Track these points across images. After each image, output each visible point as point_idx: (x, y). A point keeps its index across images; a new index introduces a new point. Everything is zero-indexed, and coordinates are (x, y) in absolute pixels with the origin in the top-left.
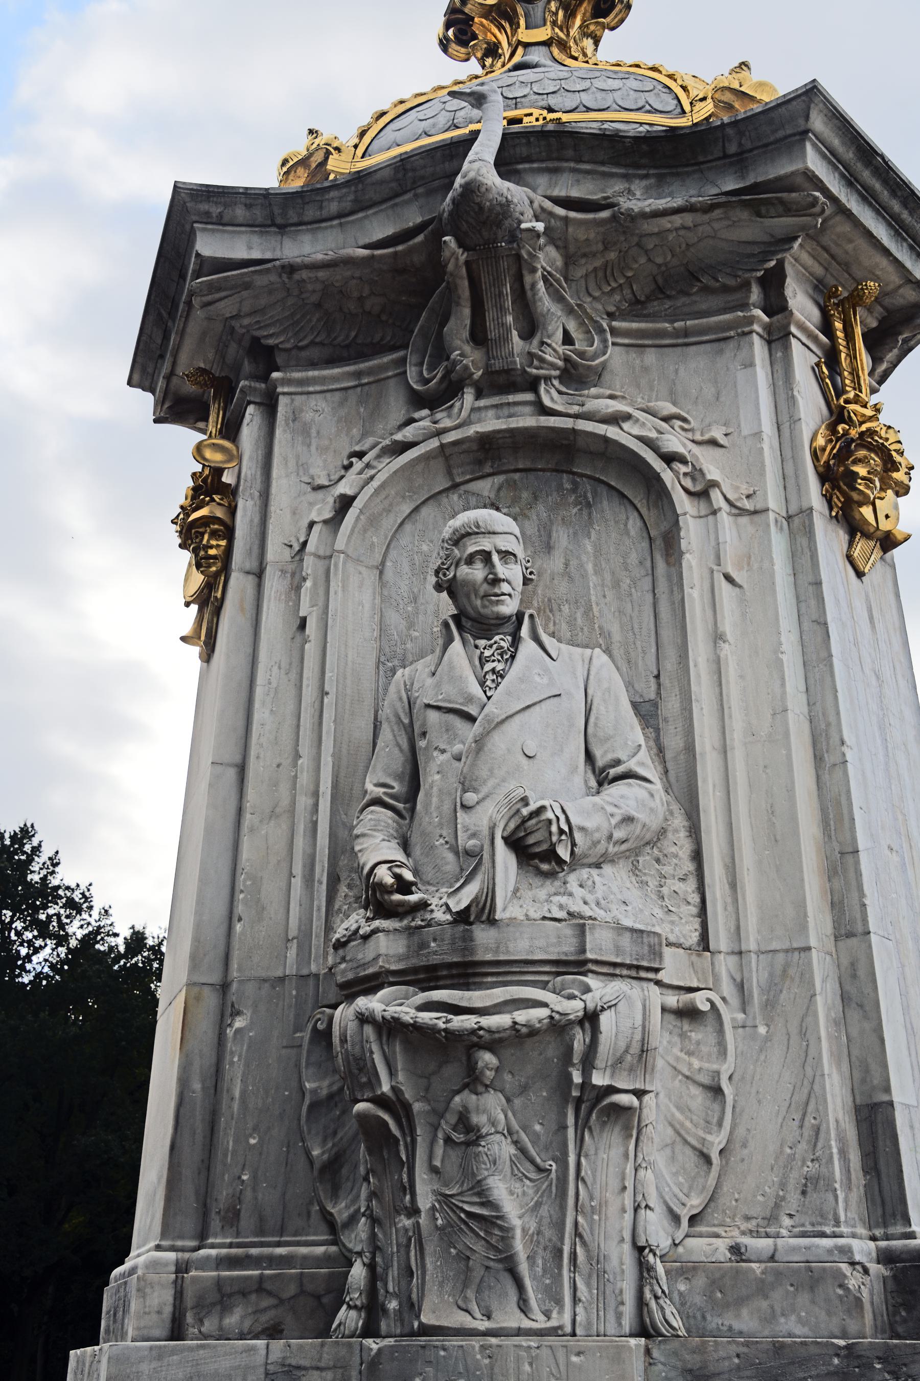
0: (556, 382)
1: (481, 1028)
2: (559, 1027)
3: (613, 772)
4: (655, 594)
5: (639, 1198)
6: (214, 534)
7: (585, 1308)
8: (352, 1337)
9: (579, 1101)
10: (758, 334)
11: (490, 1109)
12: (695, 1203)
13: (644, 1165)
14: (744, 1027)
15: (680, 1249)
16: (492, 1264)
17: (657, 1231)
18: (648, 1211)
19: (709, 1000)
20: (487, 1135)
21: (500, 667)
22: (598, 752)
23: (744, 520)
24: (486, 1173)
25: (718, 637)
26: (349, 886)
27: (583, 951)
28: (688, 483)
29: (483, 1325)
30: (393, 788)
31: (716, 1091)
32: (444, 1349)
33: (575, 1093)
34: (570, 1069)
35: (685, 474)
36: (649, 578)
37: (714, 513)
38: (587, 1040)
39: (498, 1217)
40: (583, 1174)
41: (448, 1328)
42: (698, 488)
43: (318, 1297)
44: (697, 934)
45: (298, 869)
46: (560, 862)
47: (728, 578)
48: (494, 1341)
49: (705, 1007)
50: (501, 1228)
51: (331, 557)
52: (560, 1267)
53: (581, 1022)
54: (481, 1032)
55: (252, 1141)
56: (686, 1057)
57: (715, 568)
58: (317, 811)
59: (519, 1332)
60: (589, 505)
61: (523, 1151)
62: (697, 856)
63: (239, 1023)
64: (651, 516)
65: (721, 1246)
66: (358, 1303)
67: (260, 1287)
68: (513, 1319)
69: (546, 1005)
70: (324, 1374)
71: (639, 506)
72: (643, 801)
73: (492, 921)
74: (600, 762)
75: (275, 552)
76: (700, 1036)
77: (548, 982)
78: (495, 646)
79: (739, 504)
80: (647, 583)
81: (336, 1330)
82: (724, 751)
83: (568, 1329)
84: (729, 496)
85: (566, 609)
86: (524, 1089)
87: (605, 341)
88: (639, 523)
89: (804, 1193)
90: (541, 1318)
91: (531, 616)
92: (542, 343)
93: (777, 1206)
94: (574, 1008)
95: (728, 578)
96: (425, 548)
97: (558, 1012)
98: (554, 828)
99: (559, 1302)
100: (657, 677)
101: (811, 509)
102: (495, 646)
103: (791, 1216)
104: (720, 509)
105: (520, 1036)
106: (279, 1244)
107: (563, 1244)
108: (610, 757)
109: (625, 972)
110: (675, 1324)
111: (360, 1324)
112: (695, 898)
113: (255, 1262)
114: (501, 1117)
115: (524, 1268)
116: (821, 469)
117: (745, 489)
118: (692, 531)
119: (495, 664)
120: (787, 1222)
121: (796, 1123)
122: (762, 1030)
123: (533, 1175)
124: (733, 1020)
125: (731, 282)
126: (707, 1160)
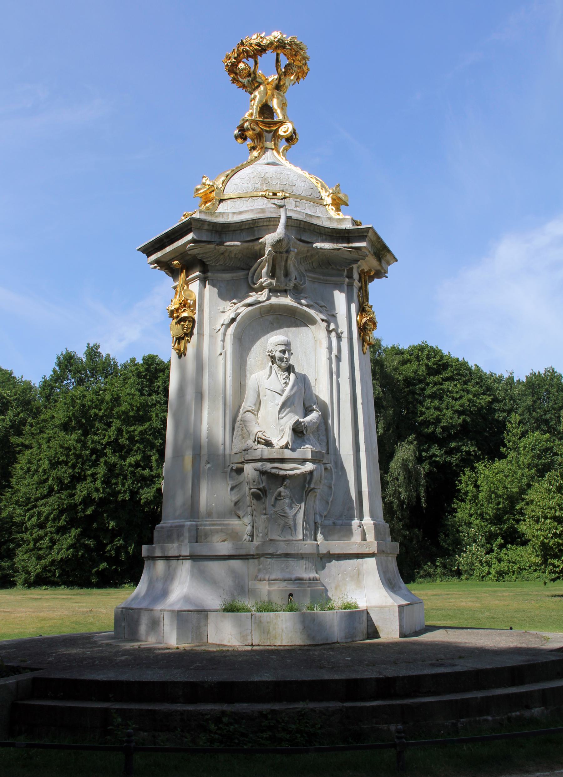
12: (325, 513)
46: (304, 434)
49: (329, 468)
65: (331, 522)
67: (222, 530)
87: (305, 279)
112: (326, 441)
113: (220, 525)
120: (344, 517)
122: (340, 473)
125: (340, 268)
126: (328, 503)
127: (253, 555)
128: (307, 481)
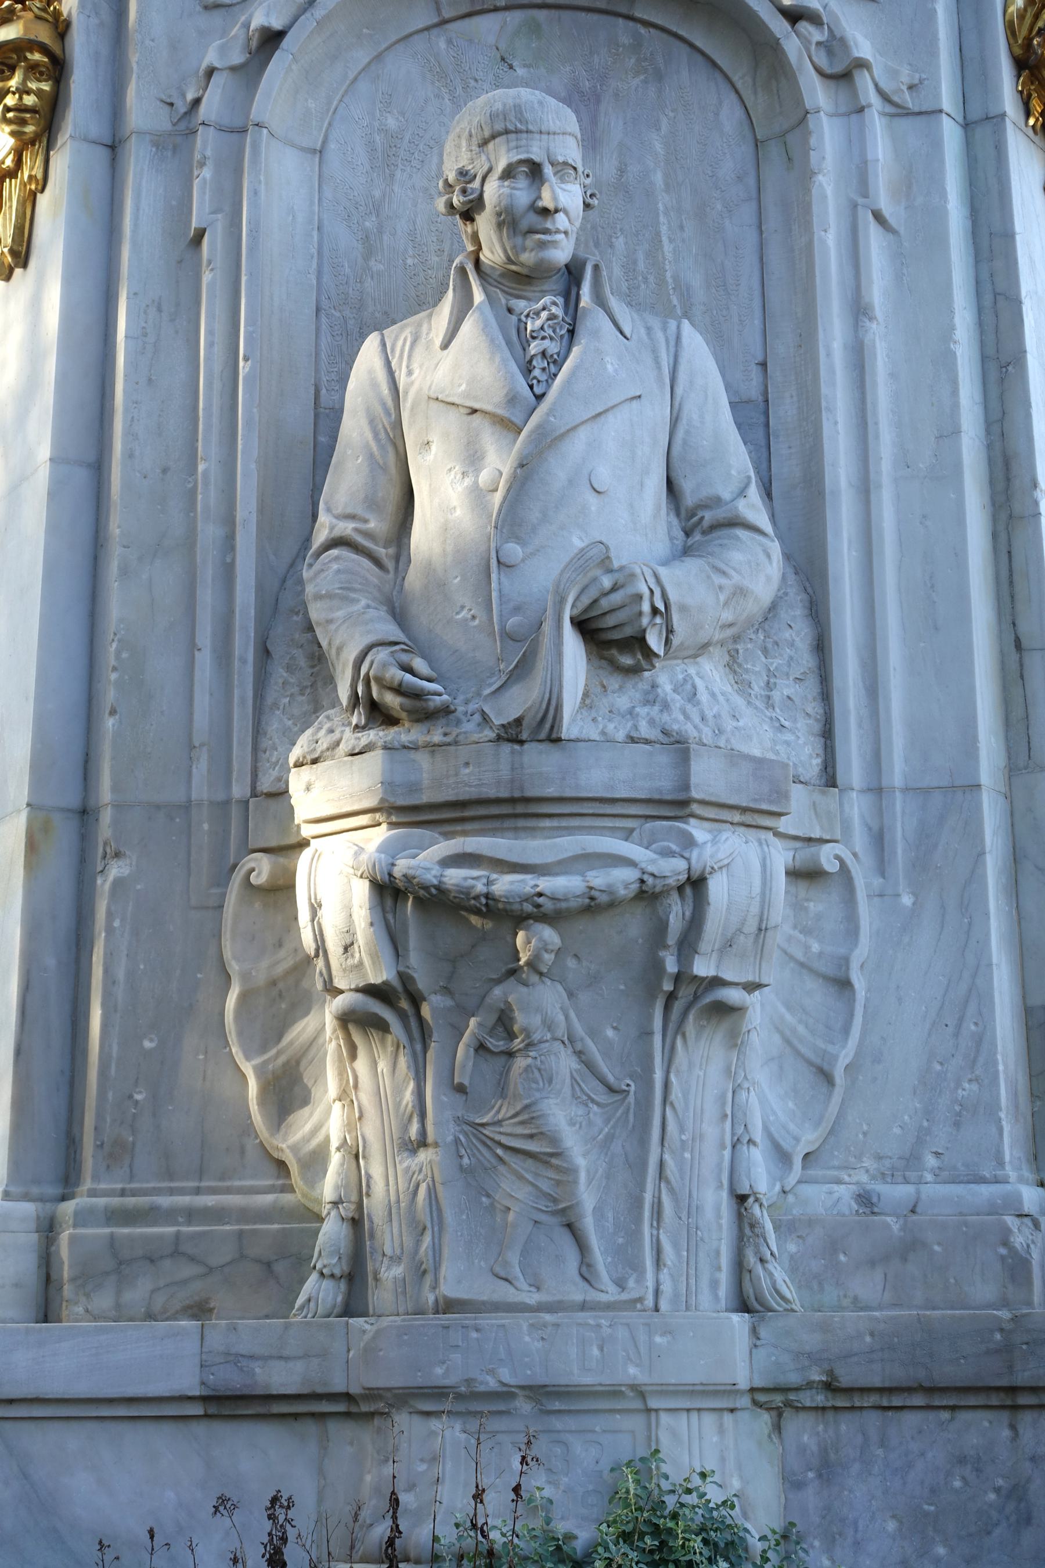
1: (540, 895)
2: (647, 895)
3: (709, 516)
4: (761, 232)
5: (740, 1130)
6: (33, 68)
7: (671, 1275)
9: (671, 997)
11: (541, 1006)
12: (809, 1139)
13: (746, 1085)
14: (881, 895)
15: (791, 1198)
16: (542, 1217)
17: (760, 1175)
18: (752, 1147)
19: (837, 857)
20: (541, 1042)
21: (553, 348)
22: (688, 487)
23: (905, 123)
24: (538, 1095)
25: (859, 310)
26: (289, 668)
27: (686, 787)
29: (532, 1298)
30: (366, 521)
31: (843, 984)
32: (477, 1330)
33: (668, 986)
34: (662, 954)
35: (819, 44)
36: (754, 204)
37: (861, 110)
38: (688, 914)
39: (552, 1155)
40: (673, 1097)
41: (484, 1303)
43: (268, 1265)
44: (819, 761)
45: (205, 637)
46: (649, 654)
47: (878, 216)
48: (548, 1317)
49: (831, 866)
50: (558, 1169)
51: (244, 131)
52: (638, 1220)
53: (680, 889)
54: (541, 900)
55: (147, 1044)
56: (801, 937)
57: (861, 201)
58: (232, 548)
59: (584, 1306)
60: (659, 77)
61: (590, 1066)
62: (822, 647)
63: (116, 870)
64: (759, 104)
65: (844, 1192)
66: (337, 1272)
67: (177, 1250)
68: (577, 1293)
69: (631, 863)
70: (291, 1364)
71: (739, 85)
72: (759, 567)
73: (554, 740)
74: (689, 500)
75: (141, 111)
76: (820, 907)
77: (632, 830)
78: (544, 315)
79: (896, 99)
80: (748, 212)
81: (302, 1308)
82: (865, 488)
83: (650, 1302)
84: (882, 85)
85: (620, 243)
86: (593, 981)
88: (739, 112)
89: (957, 1125)
90: (612, 1288)
91: (596, 268)
93: (920, 1141)
94: (673, 868)
95: (878, 216)
96: (391, 123)
97: (653, 875)
98: (646, 607)
99: (638, 1268)
100: (764, 365)
101: (1003, 115)
102: (544, 315)
103: (937, 1154)
104: (870, 106)
105: (594, 906)
106: (198, 1191)
107: (643, 1190)
108: (705, 493)
109: (737, 817)
110: (788, 1295)
111: (340, 1299)
112: (814, 708)
114: (561, 1017)
115: (589, 1224)
116: (1018, 51)
117: (906, 76)
118: (827, 137)
119: (547, 342)
120: (931, 1161)
121: (950, 1030)
123: (603, 1097)
124: (868, 886)
126: (826, 1077)
127: (347, 1397)
128: (672, 939)
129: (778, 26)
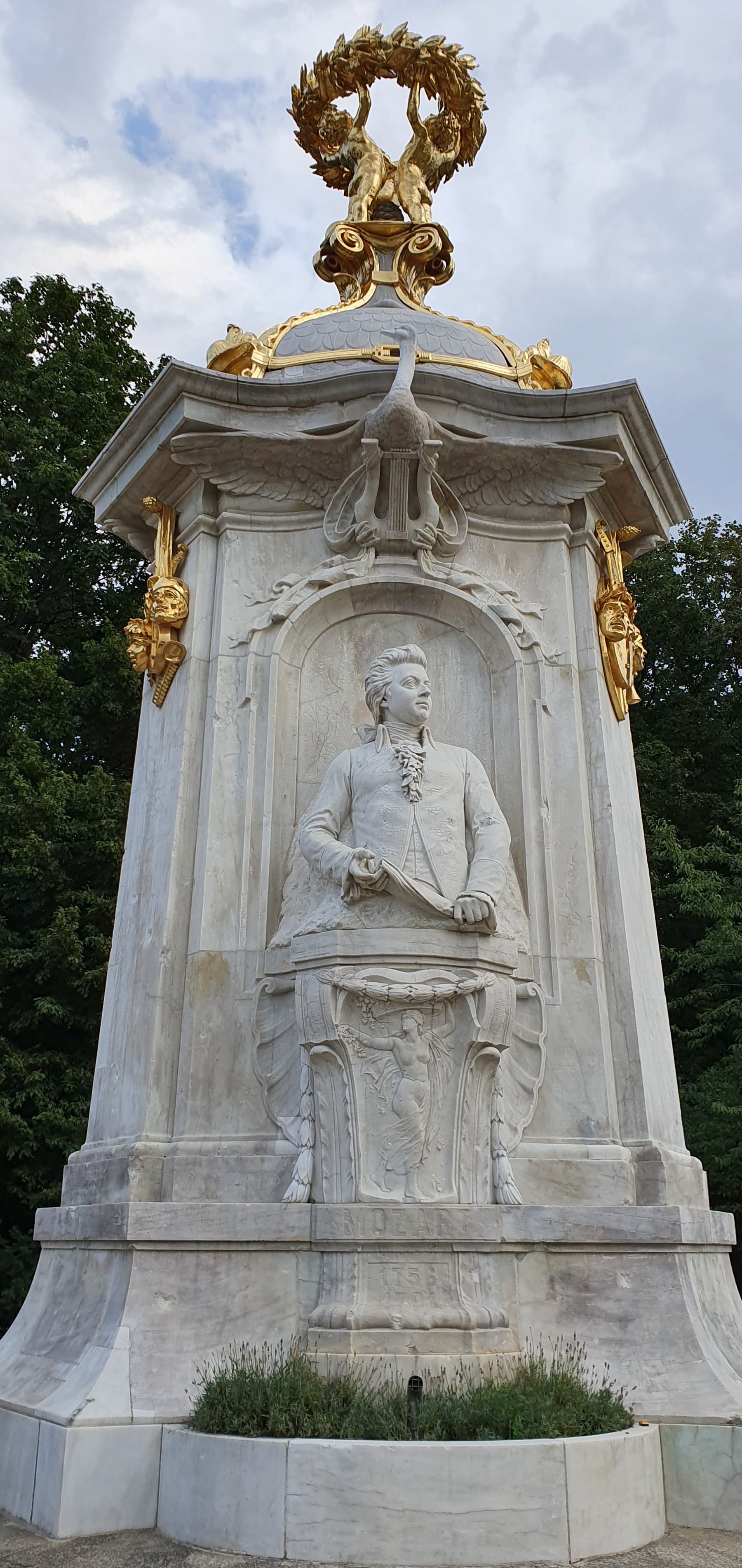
0: (430, 553)
8: (299, 1202)
10: (565, 542)
19: (533, 989)
28: (519, 640)
42: (525, 645)
47: (545, 708)
75: (224, 646)
92: (426, 525)
129: (502, 626)
